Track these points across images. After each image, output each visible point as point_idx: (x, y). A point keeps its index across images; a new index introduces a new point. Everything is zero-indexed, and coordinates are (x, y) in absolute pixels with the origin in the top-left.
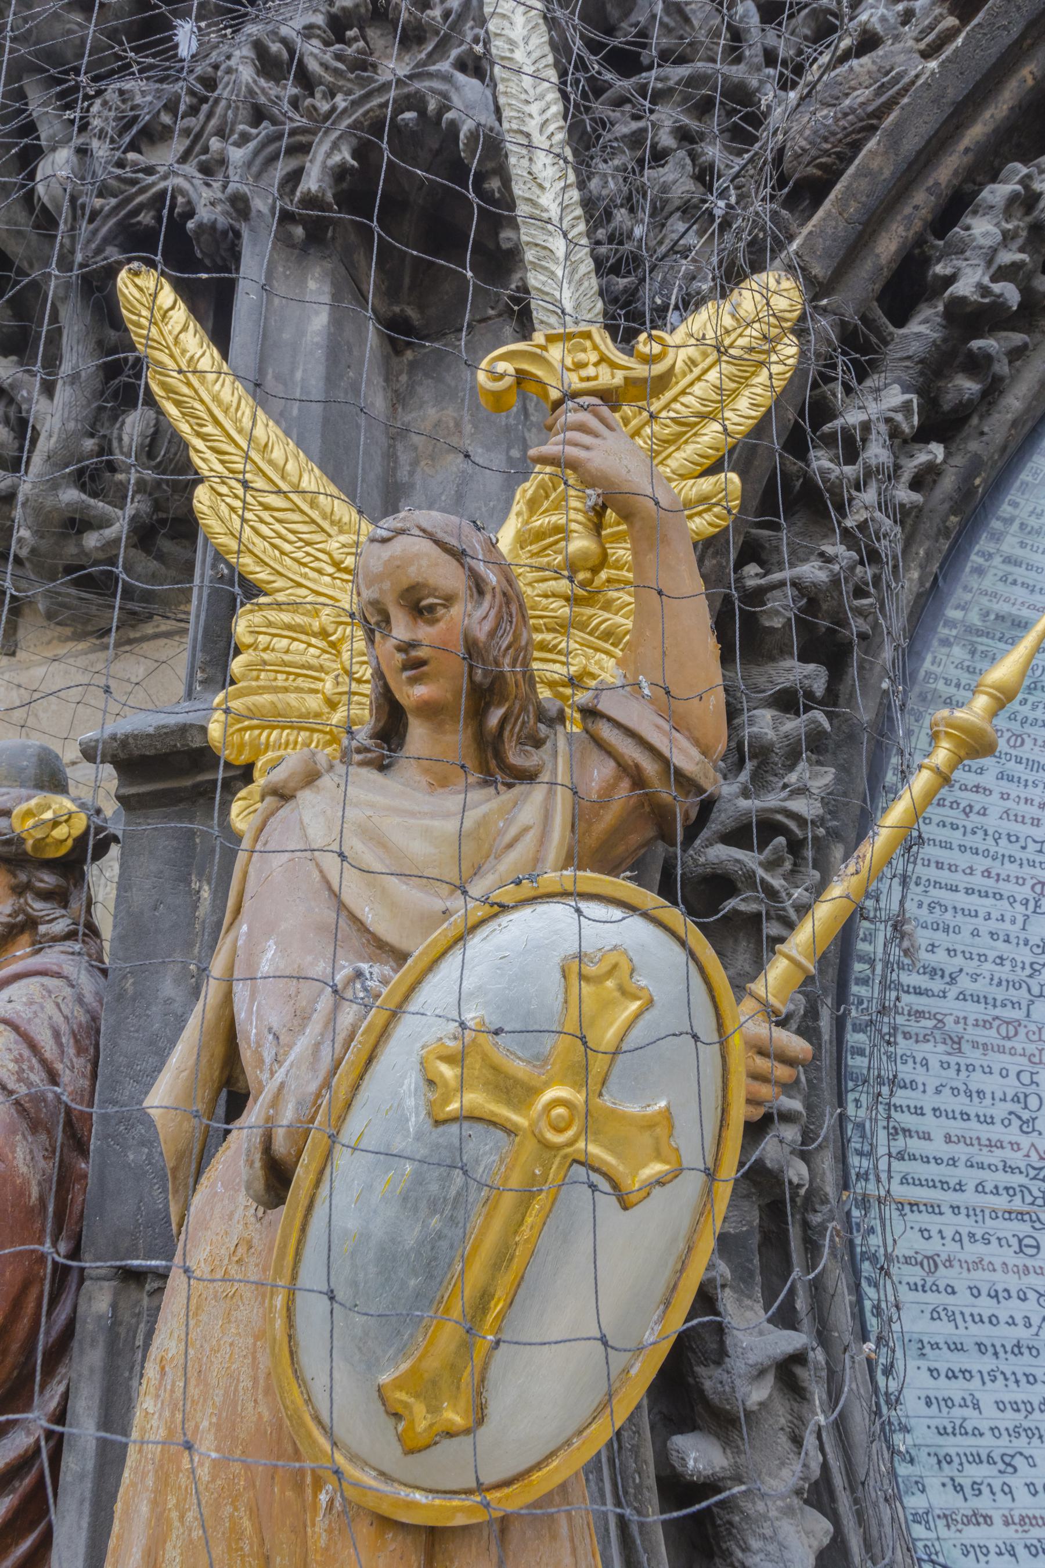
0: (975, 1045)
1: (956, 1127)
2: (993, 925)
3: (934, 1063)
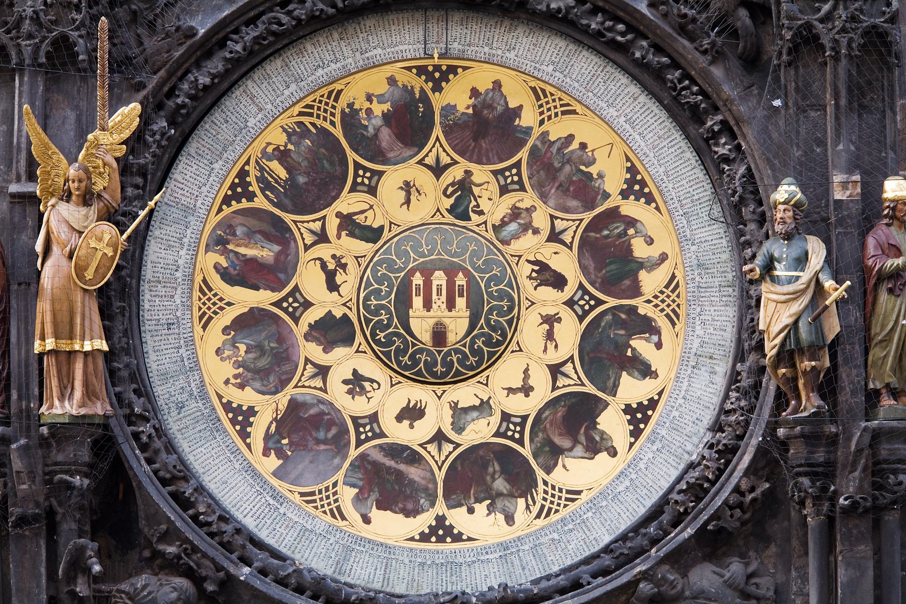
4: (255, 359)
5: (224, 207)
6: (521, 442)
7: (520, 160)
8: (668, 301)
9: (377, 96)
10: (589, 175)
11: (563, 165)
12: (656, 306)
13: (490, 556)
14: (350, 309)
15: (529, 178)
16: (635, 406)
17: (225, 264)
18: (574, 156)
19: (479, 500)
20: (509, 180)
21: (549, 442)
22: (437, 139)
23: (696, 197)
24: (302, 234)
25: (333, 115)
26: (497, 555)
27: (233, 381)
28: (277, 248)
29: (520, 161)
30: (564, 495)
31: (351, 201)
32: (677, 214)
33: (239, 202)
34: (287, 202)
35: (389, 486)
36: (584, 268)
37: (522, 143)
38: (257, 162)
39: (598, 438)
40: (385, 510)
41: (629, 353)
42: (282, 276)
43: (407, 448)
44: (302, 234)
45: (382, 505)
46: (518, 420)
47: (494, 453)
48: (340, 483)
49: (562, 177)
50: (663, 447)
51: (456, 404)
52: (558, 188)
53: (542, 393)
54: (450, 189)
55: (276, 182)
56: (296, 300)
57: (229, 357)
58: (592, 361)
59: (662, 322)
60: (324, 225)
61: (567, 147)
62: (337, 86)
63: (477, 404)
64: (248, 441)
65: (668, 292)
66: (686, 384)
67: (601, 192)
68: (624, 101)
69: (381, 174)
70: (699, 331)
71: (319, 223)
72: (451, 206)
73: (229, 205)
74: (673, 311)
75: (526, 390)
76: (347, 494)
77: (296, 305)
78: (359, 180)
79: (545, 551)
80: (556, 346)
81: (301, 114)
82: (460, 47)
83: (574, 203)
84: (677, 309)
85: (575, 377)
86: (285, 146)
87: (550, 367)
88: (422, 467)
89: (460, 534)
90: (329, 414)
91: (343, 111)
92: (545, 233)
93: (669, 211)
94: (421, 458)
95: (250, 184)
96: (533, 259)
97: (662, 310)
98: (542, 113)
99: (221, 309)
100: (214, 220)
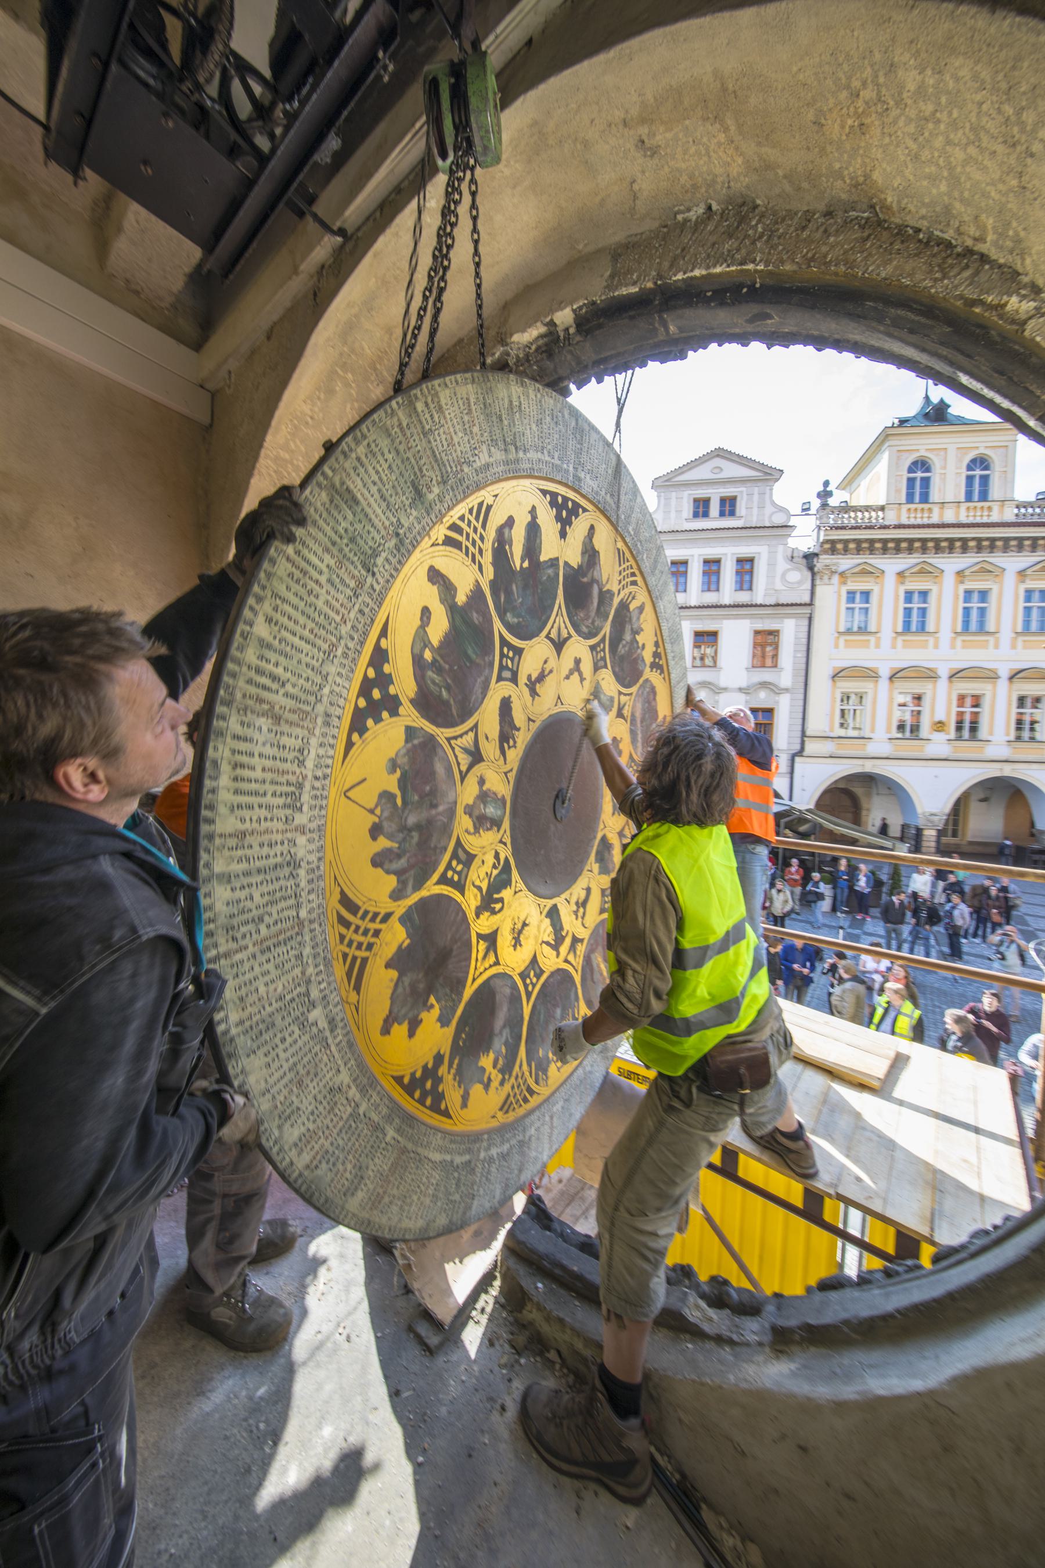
0: (287, 721)
1: (269, 763)
2: (308, 659)
3: (265, 729)
10: (402, 783)
11: (410, 830)
15: (446, 849)
32: (377, 588)
37: (423, 905)
54: (498, 906)
61: (389, 851)
67: (409, 745)
68: (266, 850)
82: (387, 1128)
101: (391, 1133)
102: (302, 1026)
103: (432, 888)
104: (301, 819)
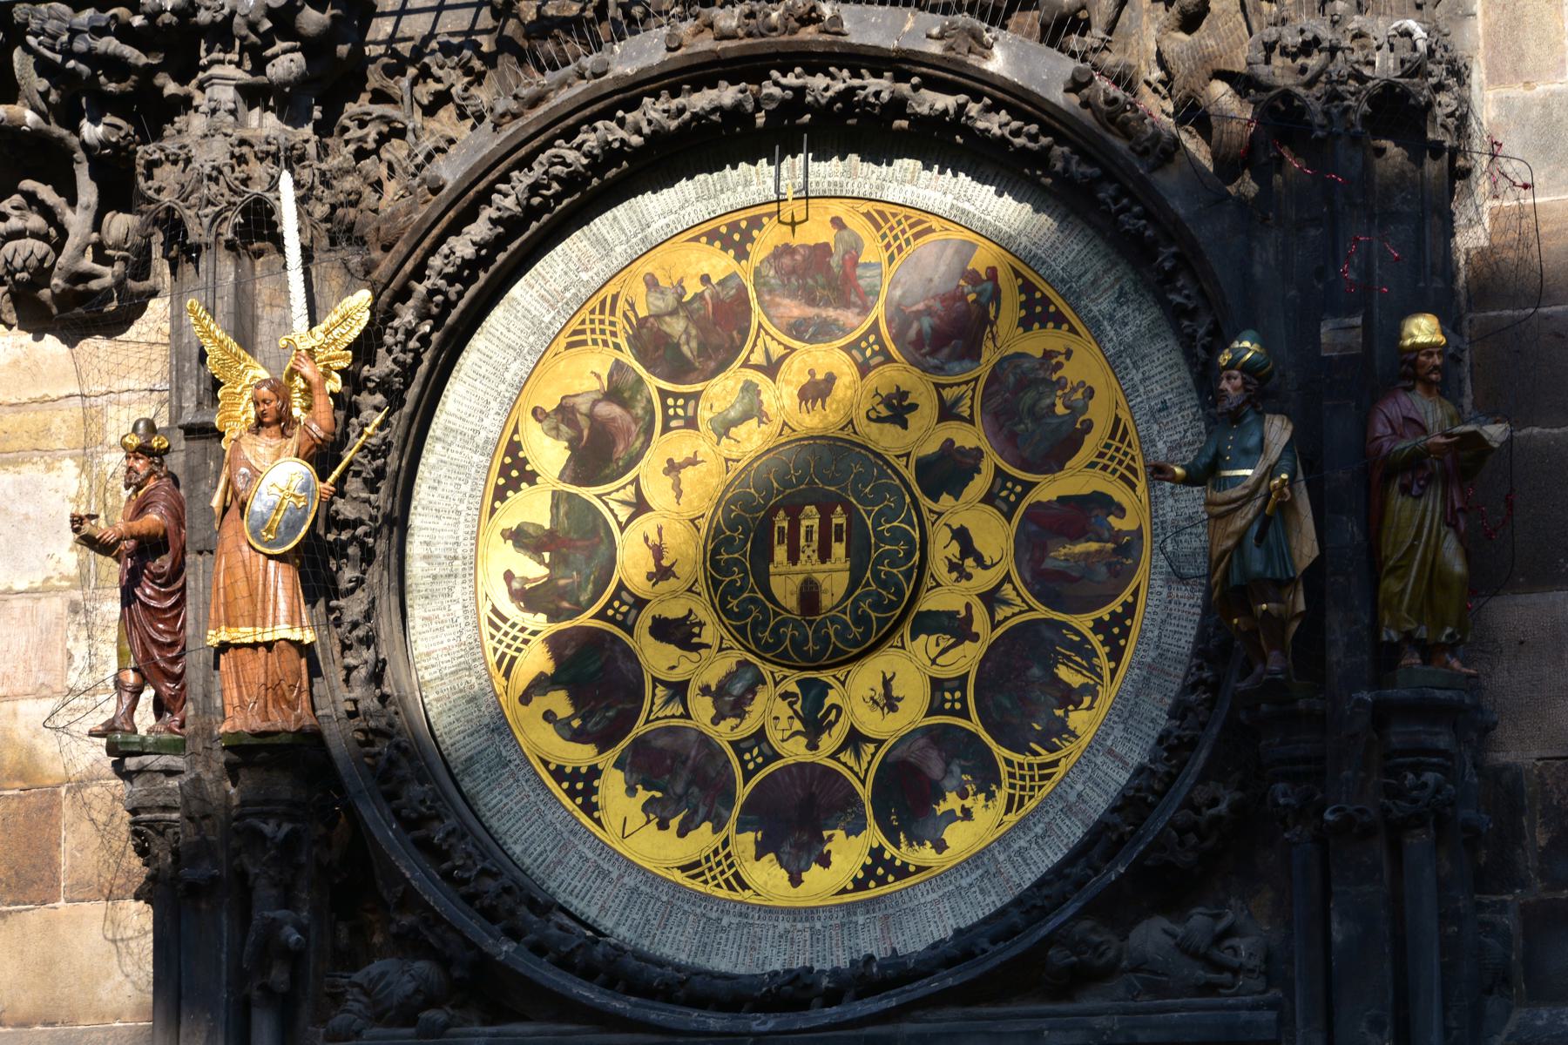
4: (1040, 399)
5: (1130, 599)
6: (664, 394)
7: (745, 783)
8: (508, 640)
9: (956, 819)
10: (647, 788)
11: (686, 792)
12: (523, 630)
13: (663, 222)
14: (931, 511)
15: (729, 761)
16: (524, 485)
17: (1111, 519)
18: (672, 807)
19: (699, 297)
20: (756, 751)
21: (625, 404)
22: (863, 782)
23: (496, 792)
24: (1019, 595)
25: (1012, 775)
26: (654, 226)
27: (1061, 358)
28: (1048, 564)
29: (746, 782)
30: (588, 337)
31: (963, 661)
33: (1113, 614)
34: (1047, 633)
35: (821, 279)
36: (631, 655)
38: (1101, 677)
39: (563, 428)
40: (817, 245)
41: (546, 555)
42: (1033, 528)
43: (812, 340)
44: (1019, 595)
45: (823, 250)
46: (673, 424)
47: (696, 369)
48: (885, 264)
49: (685, 775)
50: (472, 438)
51: (760, 422)
52: (688, 757)
53: (650, 471)
54: (832, 716)
55: (1069, 658)
56: (1006, 499)
57: (1074, 390)
58: (594, 531)
59: (511, 610)
60: (992, 617)
61: (685, 818)
62: (1013, 818)
63: (733, 430)
64: (1020, 281)
65: (511, 652)
66: (461, 533)
69: (930, 712)
70: (457, 609)
71: (999, 617)
72: (826, 694)
73: (1125, 604)
74: (498, 628)
75: (673, 468)
76: (872, 251)
77: (1004, 493)
78: (958, 694)
79: (593, 251)
80: (646, 539)
81: (1055, 763)
82: (854, 919)
83: (661, 742)
84: (494, 632)
85: (613, 505)
86: (1067, 712)
87: (650, 509)
88: (785, 321)
89: (710, 242)
90: (924, 356)
91: (999, 786)
92: (693, 691)
93: (529, 763)
94: (789, 334)
95: (1104, 643)
96: (702, 651)
97: (513, 625)
98: (728, 856)
99: (1101, 455)
100: (1141, 576)
101: (861, 920)
102: (723, 930)
103: (743, 792)
104: (614, 875)
